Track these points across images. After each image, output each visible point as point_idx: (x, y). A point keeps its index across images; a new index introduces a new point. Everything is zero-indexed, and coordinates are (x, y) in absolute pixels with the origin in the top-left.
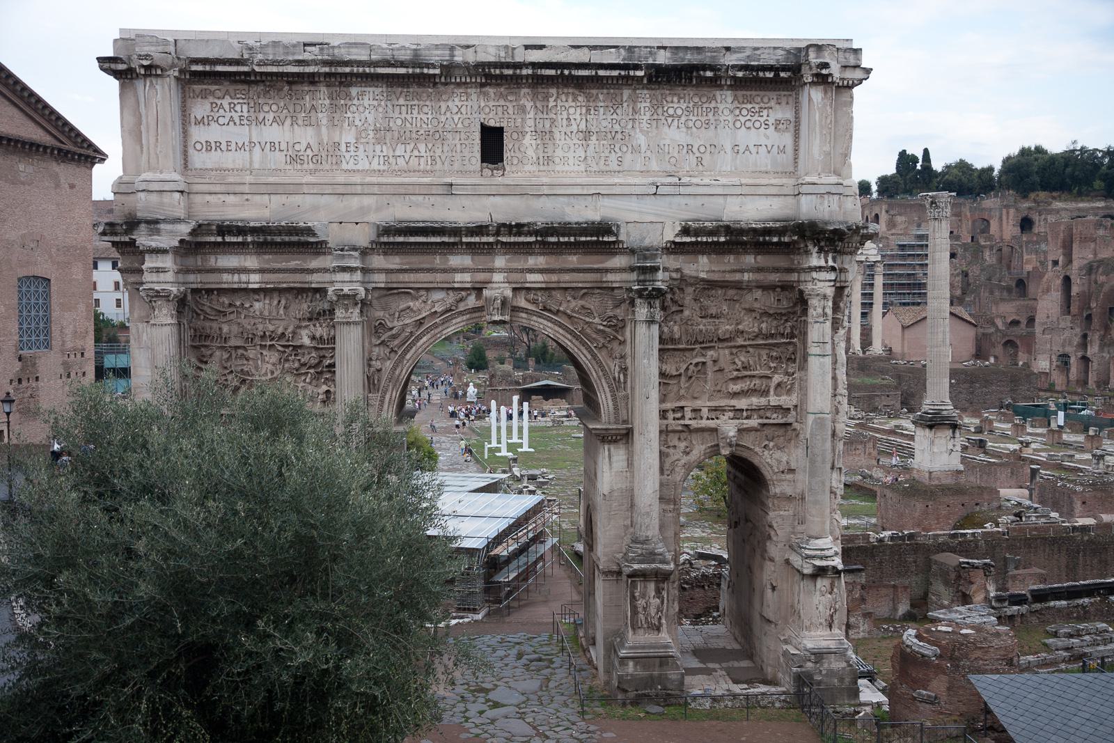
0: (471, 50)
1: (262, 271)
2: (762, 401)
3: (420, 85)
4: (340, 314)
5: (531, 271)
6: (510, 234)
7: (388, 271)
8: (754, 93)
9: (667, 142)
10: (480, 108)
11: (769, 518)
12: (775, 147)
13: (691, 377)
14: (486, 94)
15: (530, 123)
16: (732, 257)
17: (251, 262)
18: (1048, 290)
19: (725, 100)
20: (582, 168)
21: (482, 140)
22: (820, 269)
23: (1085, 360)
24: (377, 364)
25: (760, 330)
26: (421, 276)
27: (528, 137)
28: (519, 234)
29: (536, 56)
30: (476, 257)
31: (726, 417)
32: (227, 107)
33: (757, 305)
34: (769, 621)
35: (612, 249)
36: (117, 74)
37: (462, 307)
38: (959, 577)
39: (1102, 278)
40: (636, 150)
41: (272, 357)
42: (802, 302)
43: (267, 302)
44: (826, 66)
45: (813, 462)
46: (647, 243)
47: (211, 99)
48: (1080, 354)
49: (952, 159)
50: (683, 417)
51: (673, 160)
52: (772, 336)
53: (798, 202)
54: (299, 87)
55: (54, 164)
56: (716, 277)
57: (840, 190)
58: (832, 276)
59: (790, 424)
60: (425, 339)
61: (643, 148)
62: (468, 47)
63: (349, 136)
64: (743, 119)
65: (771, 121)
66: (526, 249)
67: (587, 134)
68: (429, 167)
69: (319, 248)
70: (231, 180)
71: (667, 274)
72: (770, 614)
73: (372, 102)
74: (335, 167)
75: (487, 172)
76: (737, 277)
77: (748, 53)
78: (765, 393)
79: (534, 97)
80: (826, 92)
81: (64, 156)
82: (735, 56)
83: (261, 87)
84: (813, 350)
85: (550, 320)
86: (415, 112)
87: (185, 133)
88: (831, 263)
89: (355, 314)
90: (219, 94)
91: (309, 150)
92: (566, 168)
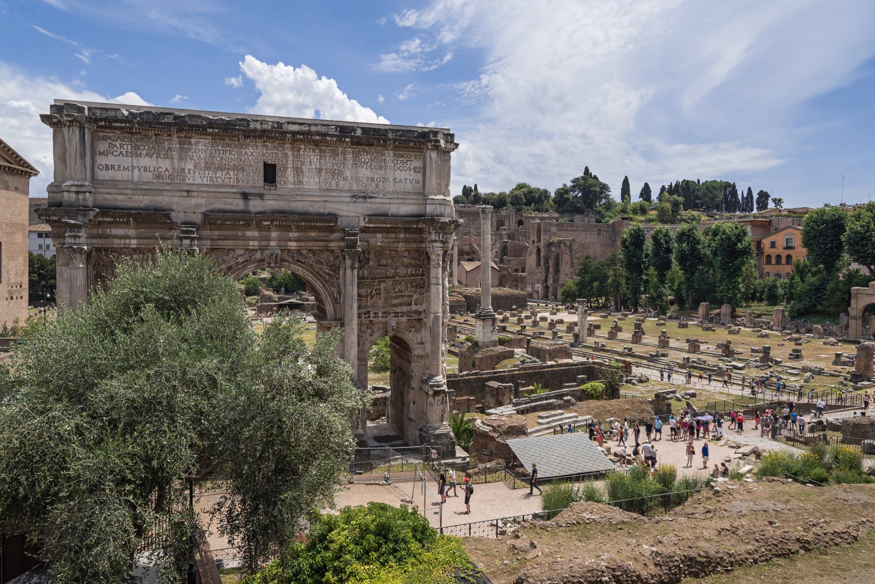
0: (259, 123)
1: (138, 238)
3: (230, 140)
5: (290, 241)
7: (212, 240)
9: (361, 175)
10: (264, 154)
11: (412, 367)
15: (290, 162)
16: (393, 235)
17: (132, 232)
18: (531, 254)
20: (318, 187)
21: (265, 170)
22: (436, 241)
25: (407, 272)
26: (231, 242)
27: (289, 170)
30: (261, 233)
31: (390, 317)
32: (118, 146)
35: (332, 230)
36: (51, 124)
37: (253, 257)
43: (141, 255)
47: (109, 141)
50: (369, 317)
52: (413, 275)
53: (425, 208)
54: (162, 137)
55: (5, 175)
56: (385, 245)
57: (445, 202)
59: (422, 319)
61: (349, 178)
62: (257, 121)
63: (190, 166)
64: (398, 166)
65: (412, 167)
67: (320, 171)
68: (235, 184)
70: (120, 186)
72: (412, 416)
73: (203, 147)
74: (182, 182)
75: (267, 187)
77: (401, 133)
79: (293, 149)
81: (12, 171)
83: (139, 136)
84: (433, 281)
85: (301, 266)
86: (228, 154)
90: (114, 138)
91: (167, 173)
92: (309, 187)
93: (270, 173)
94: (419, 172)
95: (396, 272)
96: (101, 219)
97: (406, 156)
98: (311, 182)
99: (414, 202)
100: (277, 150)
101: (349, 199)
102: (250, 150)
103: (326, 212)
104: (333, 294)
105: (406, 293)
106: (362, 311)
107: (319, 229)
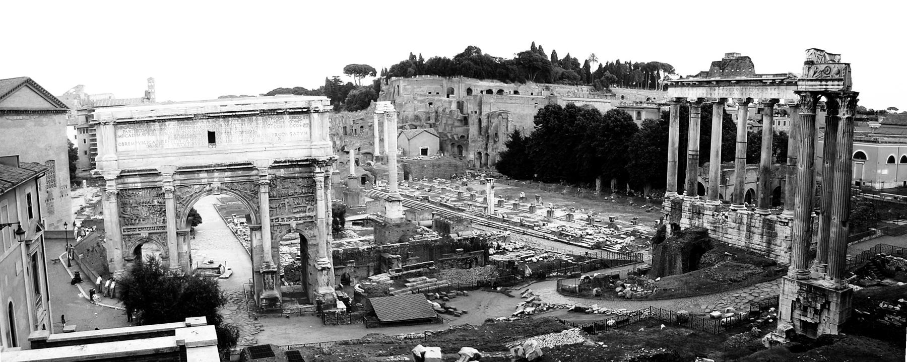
1: (141, 183)
2: (304, 214)
4: (166, 195)
5: (226, 177)
6: (219, 166)
7: (181, 180)
10: (207, 126)
17: (137, 179)
23: (487, 155)
24: (179, 210)
27: (223, 134)
28: (222, 166)
33: (300, 184)
35: (252, 169)
38: (389, 262)
40: (258, 136)
41: (145, 209)
42: (314, 182)
44: (317, 107)
45: (320, 234)
46: (263, 166)
48: (485, 152)
52: (306, 193)
53: (311, 152)
58: (323, 174)
63: (165, 138)
65: (302, 124)
66: (225, 170)
69: (158, 174)
70: (130, 155)
71: (270, 176)
72: (310, 282)
75: (211, 146)
76: (293, 175)
77: (293, 103)
78: (305, 212)
84: (318, 198)
87: (116, 140)
88: (322, 171)
89: (171, 195)
93: (212, 137)
96: (122, 174)
99: (304, 147)
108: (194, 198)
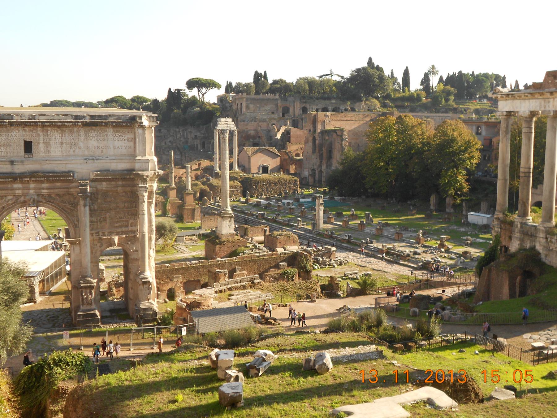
0: (19, 116)
2: (126, 229)
5: (43, 189)
8: (120, 129)
10: (23, 136)
12: (128, 147)
13: (101, 222)
14: (25, 130)
15: (42, 139)
16: (114, 183)
19: (110, 131)
23: (321, 172)
26: (3, 192)
27: (41, 144)
29: (43, 119)
30: (23, 185)
34: (131, 299)
35: (71, 181)
37: (19, 200)
39: (327, 138)
42: (137, 196)
46: (84, 178)
48: (319, 170)
49: (277, 78)
50: (99, 235)
51: (93, 151)
60: (5, 213)
61: (82, 147)
64: (116, 138)
65: (126, 138)
66: (42, 182)
67: (62, 143)
68: (5, 155)
75: (27, 156)
78: (127, 226)
79: (43, 131)
80: (143, 130)
82: (112, 118)
84: (141, 212)
88: (145, 185)
92: (55, 154)
93: (28, 147)
94: (131, 141)
95: (117, 206)
97: (121, 131)
98: (56, 151)
100: (32, 132)
101: (82, 161)
102: (14, 133)
103: (67, 170)
104: (73, 221)
105: (125, 219)
106: (93, 232)
107: (63, 181)
108: (6, 210)
